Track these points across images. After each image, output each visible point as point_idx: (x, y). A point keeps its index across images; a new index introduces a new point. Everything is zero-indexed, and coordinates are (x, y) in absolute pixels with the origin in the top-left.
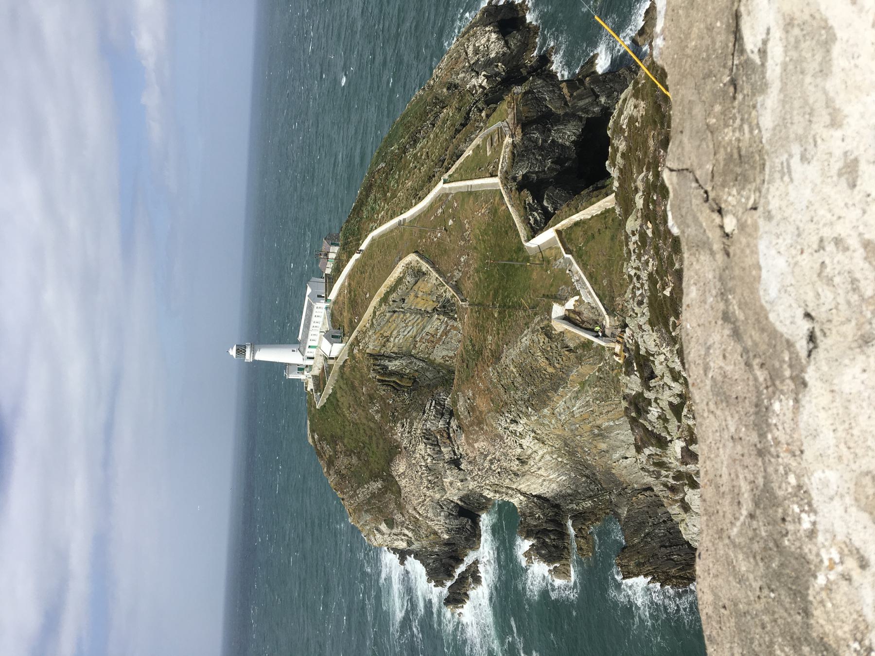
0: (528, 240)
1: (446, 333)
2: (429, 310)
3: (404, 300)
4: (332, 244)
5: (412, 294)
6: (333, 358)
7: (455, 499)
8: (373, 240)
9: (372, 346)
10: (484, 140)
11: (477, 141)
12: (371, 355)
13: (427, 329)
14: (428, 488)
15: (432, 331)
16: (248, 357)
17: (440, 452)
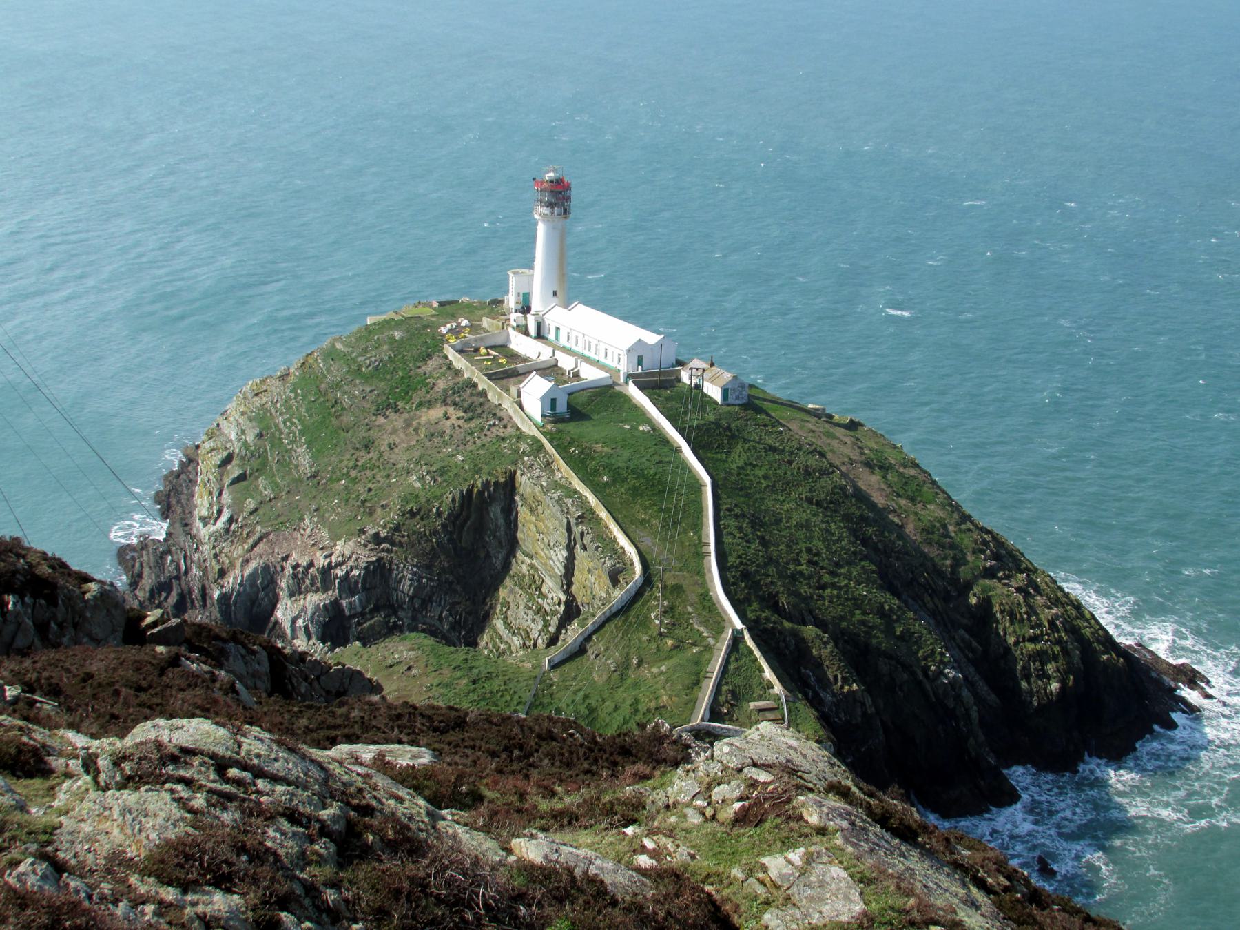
1: (539, 610)
3: (585, 549)
4: (725, 392)
6: (519, 395)
7: (279, 613)
8: (697, 487)
9: (525, 483)
10: (778, 698)
11: (778, 689)
12: (512, 477)
14: (295, 567)
15: (544, 589)
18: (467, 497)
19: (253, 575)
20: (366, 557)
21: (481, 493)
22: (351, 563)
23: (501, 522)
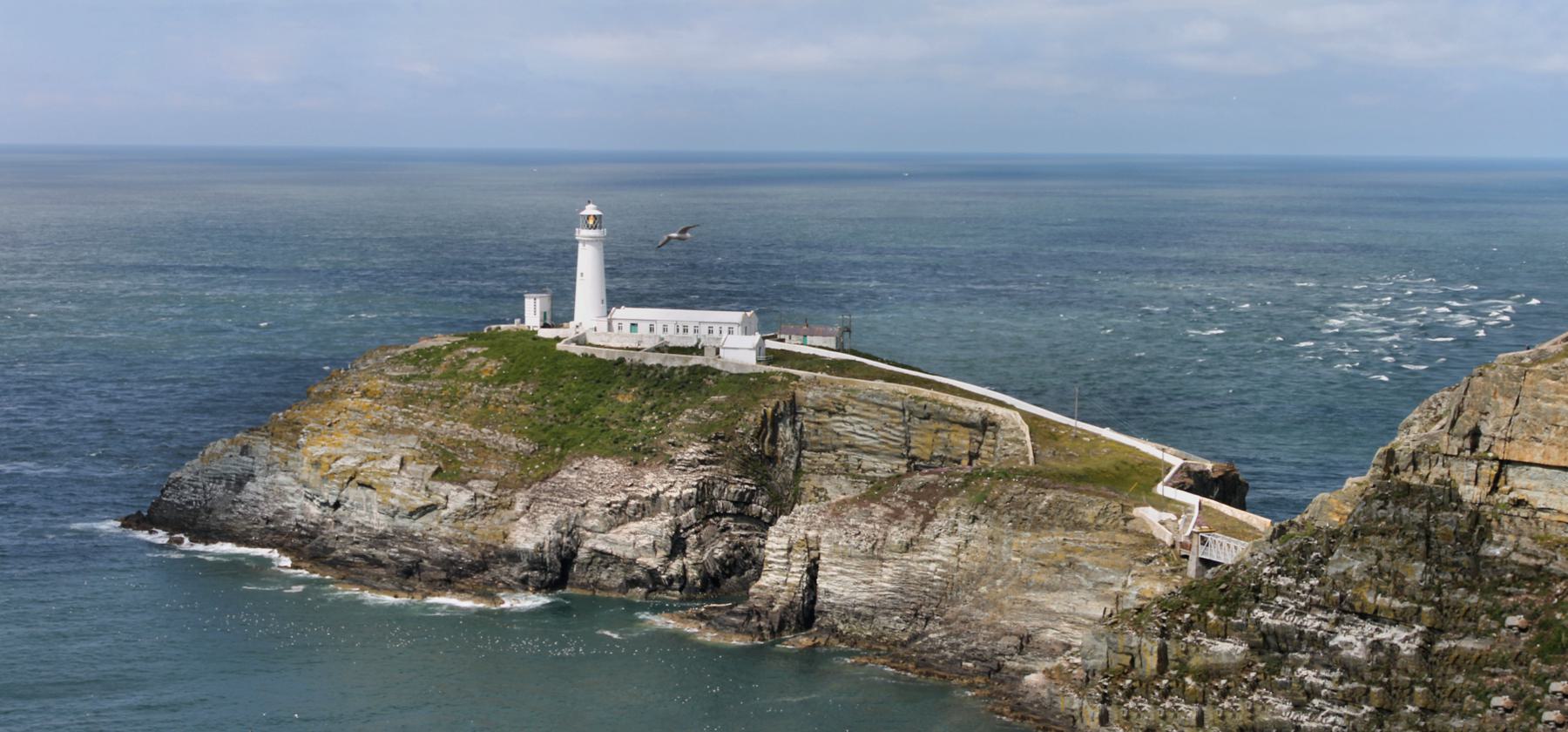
0: (1166, 484)
2: (913, 452)
3: (928, 417)
5: (942, 426)
12: (794, 396)
13: (865, 457)
15: (865, 465)
16: (583, 233)
17: (687, 508)
18: (765, 416)
19: (557, 527)
20: (692, 479)
21: (775, 411)
22: (679, 486)
23: (789, 434)
